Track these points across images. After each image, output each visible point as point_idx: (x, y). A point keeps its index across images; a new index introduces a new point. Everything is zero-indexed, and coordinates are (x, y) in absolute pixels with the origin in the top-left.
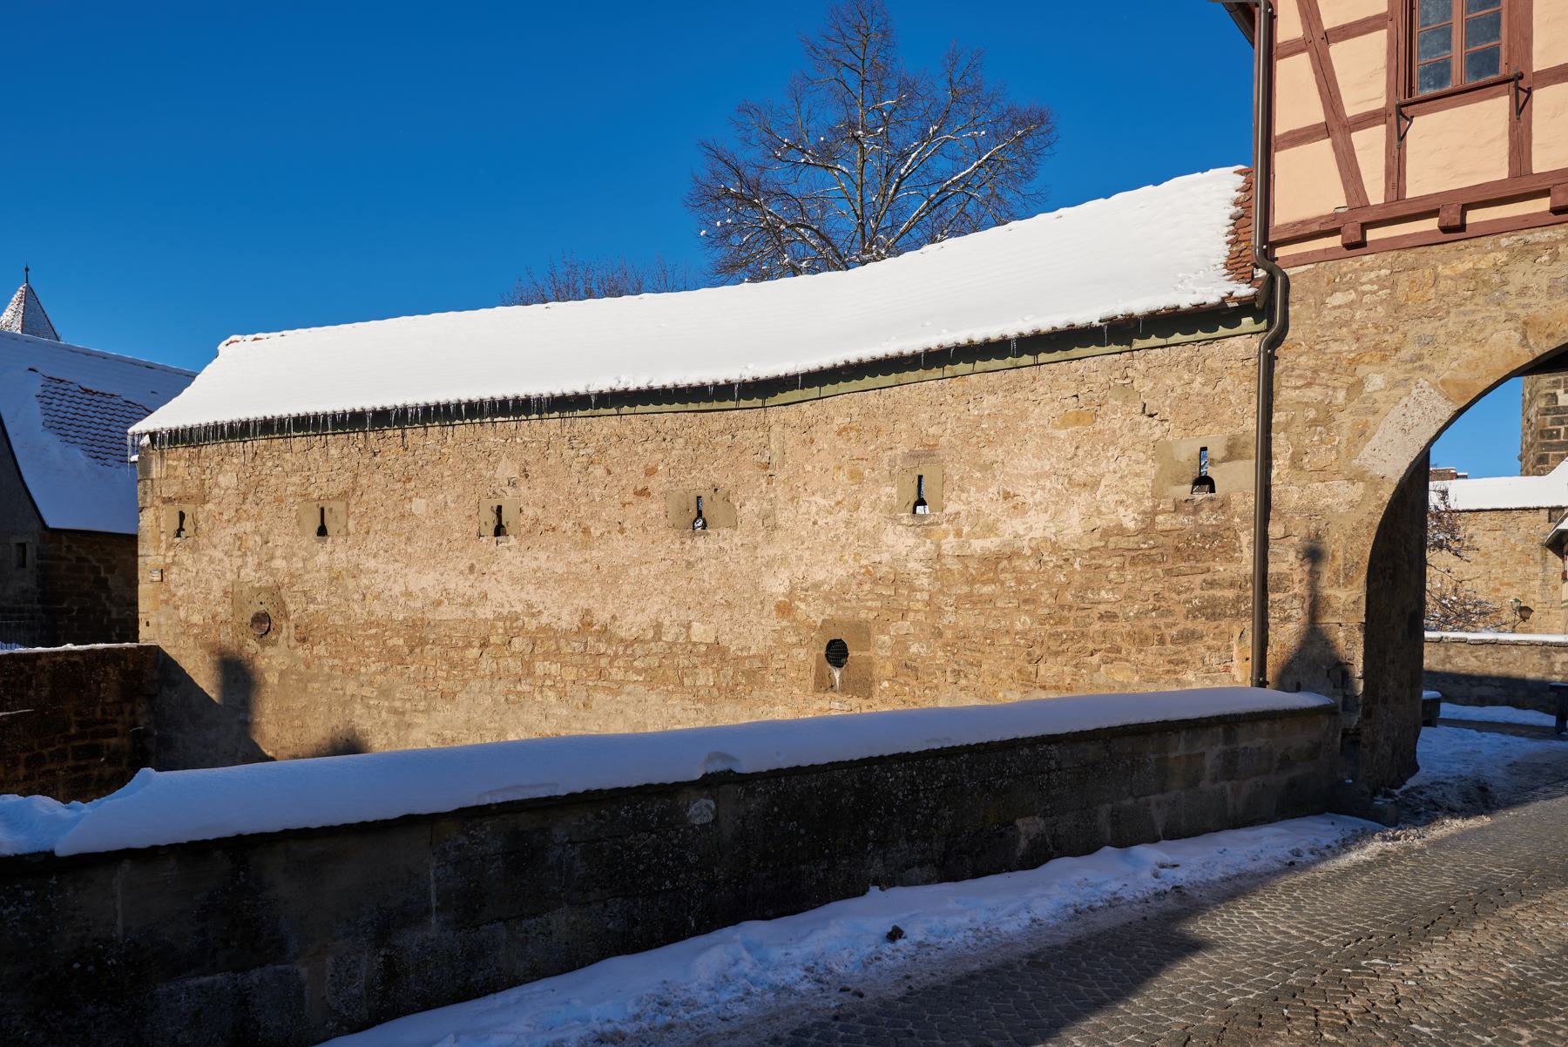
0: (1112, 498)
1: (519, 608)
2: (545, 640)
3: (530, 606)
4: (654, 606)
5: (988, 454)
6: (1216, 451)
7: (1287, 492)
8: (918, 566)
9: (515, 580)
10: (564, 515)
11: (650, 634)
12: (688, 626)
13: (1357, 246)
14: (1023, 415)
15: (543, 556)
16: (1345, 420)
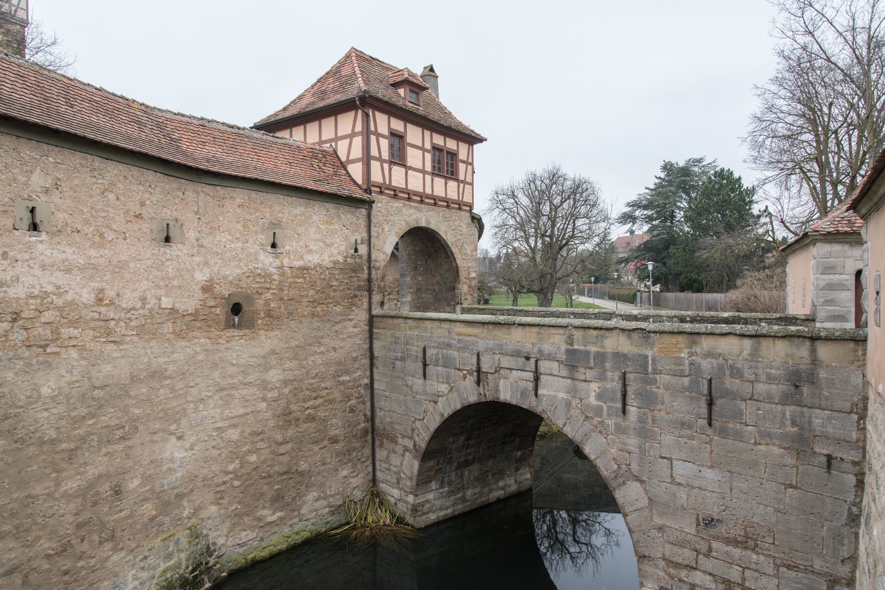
0: (336, 252)
1: (49, 288)
2: (70, 314)
3: (58, 288)
4: (144, 285)
5: (300, 230)
6: (359, 241)
7: (373, 257)
8: (274, 270)
9: (43, 267)
10: (87, 222)
11: (139, 305)
12: (160, 299)
13: (381, 192)
14: (310, 217)
15: (69, 251)
16: (381, 237)
